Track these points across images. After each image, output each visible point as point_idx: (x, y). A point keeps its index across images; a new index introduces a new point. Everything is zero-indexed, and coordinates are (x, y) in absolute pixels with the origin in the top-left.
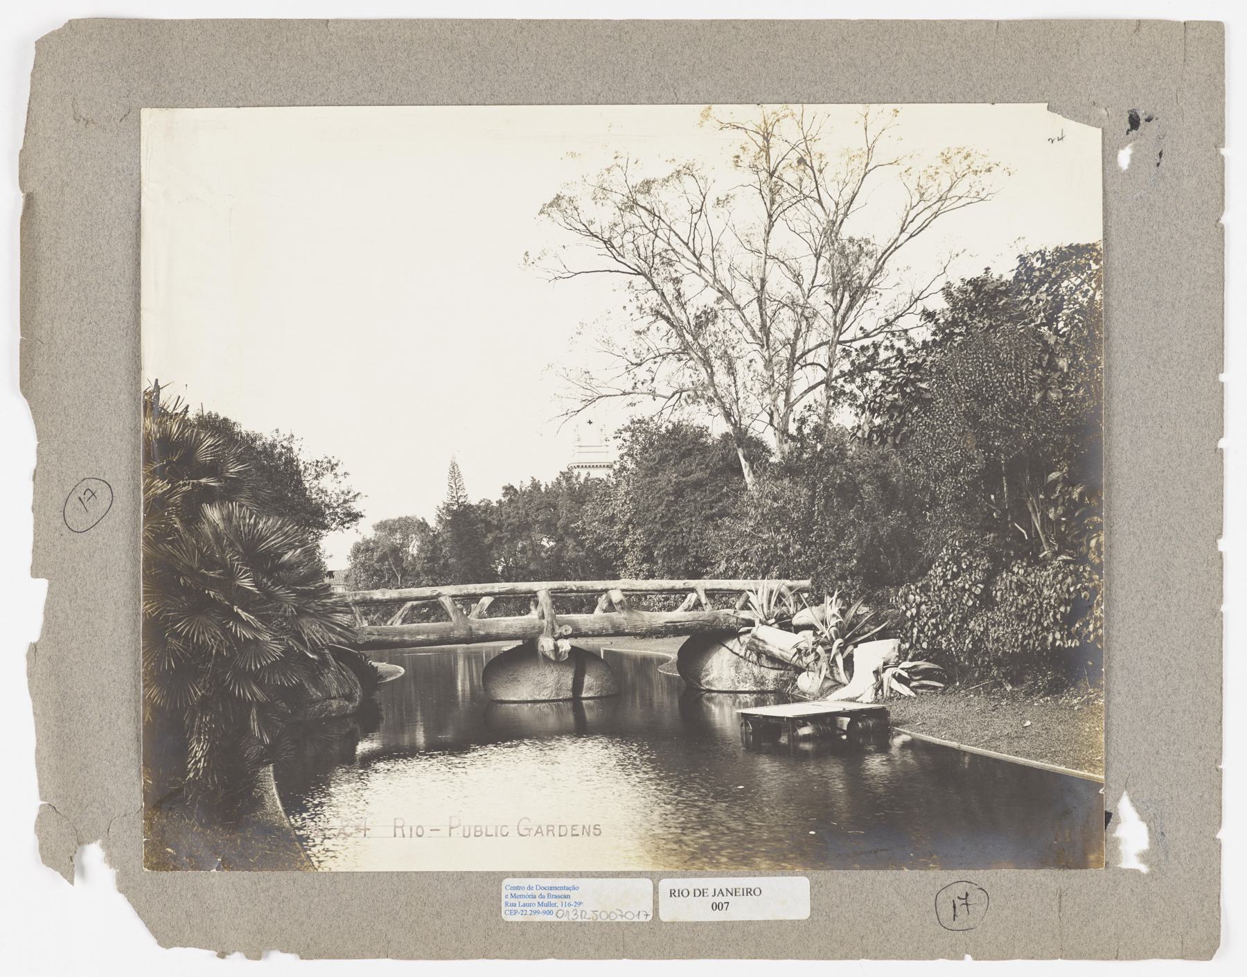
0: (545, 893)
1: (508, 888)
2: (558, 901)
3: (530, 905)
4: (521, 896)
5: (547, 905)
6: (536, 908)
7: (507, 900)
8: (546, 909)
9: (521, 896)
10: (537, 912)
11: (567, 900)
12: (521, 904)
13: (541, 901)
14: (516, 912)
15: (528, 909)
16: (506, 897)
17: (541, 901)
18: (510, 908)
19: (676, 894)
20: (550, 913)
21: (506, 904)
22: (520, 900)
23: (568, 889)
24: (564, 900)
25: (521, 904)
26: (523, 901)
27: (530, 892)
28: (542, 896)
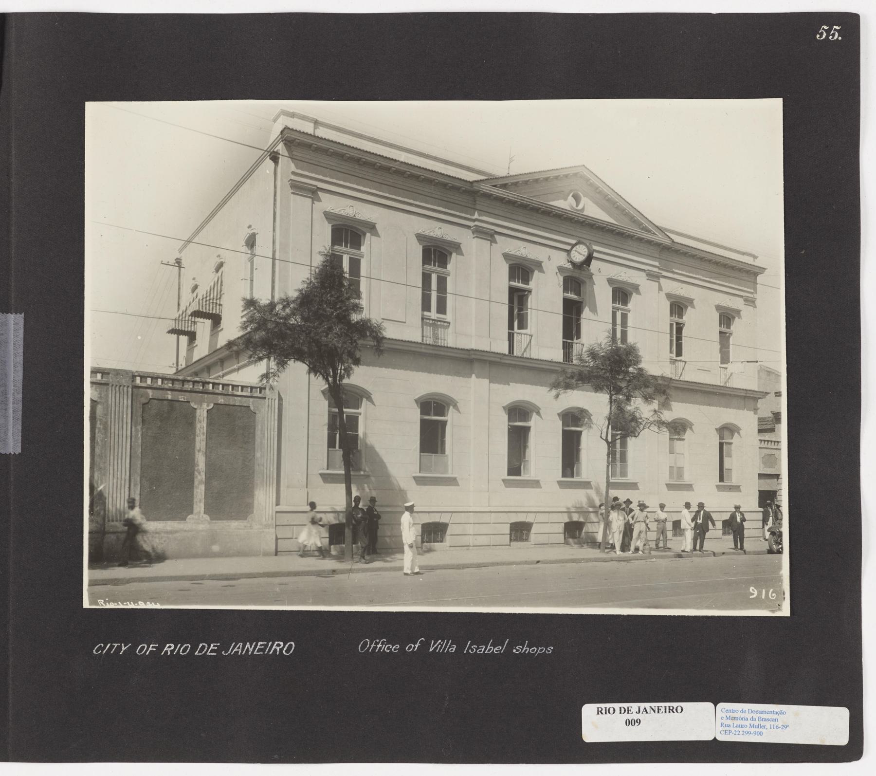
0: (756, 716)
1: (724, 710)
3: (742, 726)
7: (722, 721)
9: (734, 719)
11: (776, 723)
12: (735, 726)
14: (730, 732)
15: (741, 729)
16: (722, 718)
17: (752, 722)
20: (760, 734)
21: (722, 725)
23: (776, 713)
24: (773, 723)
25: (735, 726)
27: (743, 715)
28: (753, 719)
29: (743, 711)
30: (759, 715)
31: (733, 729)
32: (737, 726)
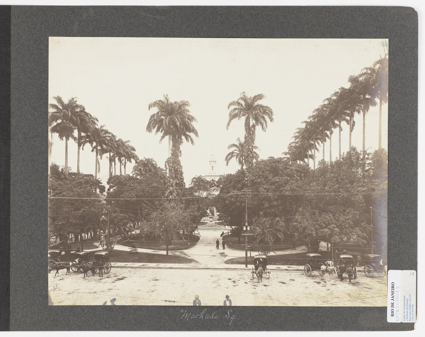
0: (406, 307)
2: (409, 303)
3: (410, 313)
4: (407, 316)
5: (410, 306)
6: (411, 310)
7: (408, 321)
8: (411, 307)
9: (407, 316)
11: (409, 299)
12: (410, 315)
13: (409, 309)
14: (412, 317)
15: (411, 313)
16: (407, 321)
17: (409, 309)
18: (411, 320)
19: (393, 314)
20: (413, 305)
21: (410, 321)
22: (408, 316)
23: (405, 299)
24: (409, 301)
25: (410, 315)
27: (406, 312)
28: (407, 308)
30: (406, 306)
31: (411, 317)
32: (410, 314)
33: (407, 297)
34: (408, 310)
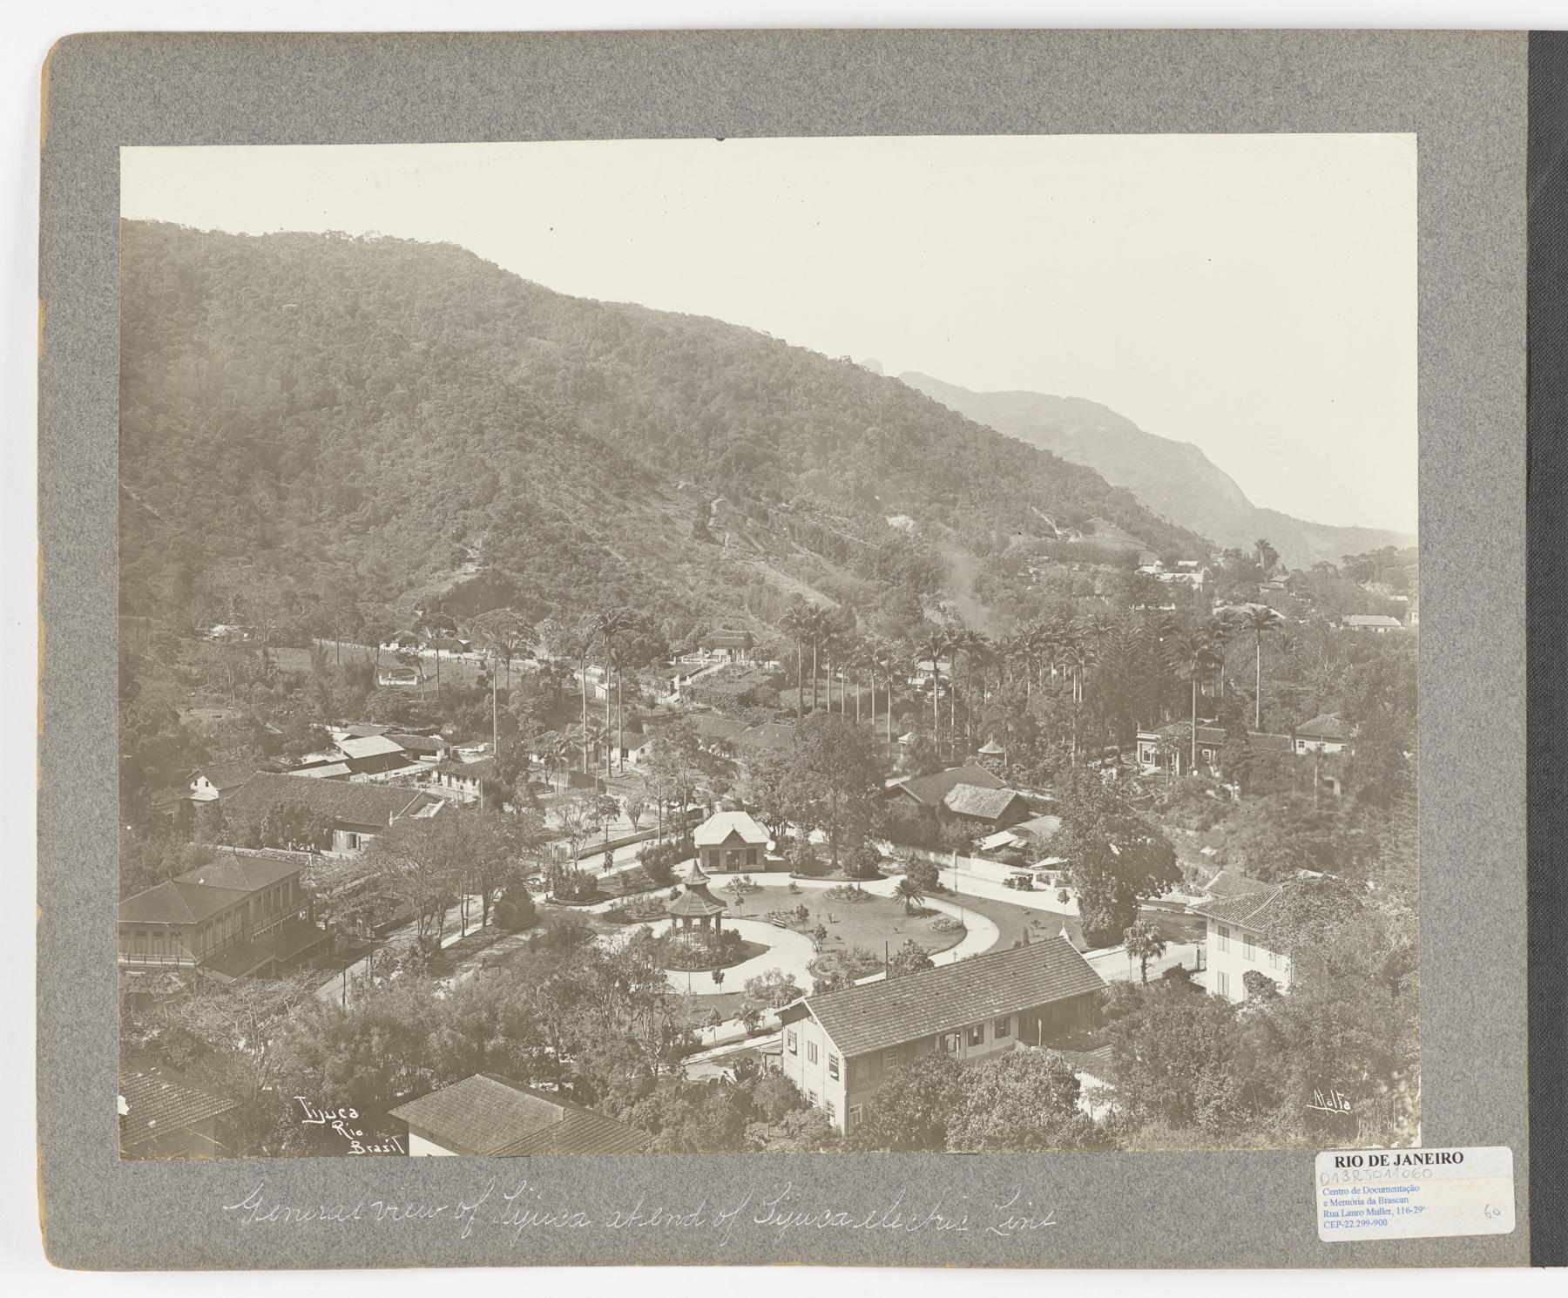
0: (1375, 1196)
2: (1393, 1207)
3: (1356, 1213)
5: (1378, 1213)
6: (1365, 1217)
10: (1366, 1222)
11: (1405, 1205)
13: (1370, 1207)
14: (1339, 1223)
15: (1354, 1219)
20: (1384, 1222)
21: (1326, 1214)
23: (1405, 1190)
24: (1400, 1205)
26: (1348, 1208)
27: (1356, 1197)
28: (1372, 1202)
29: (1355, 1191)
30: (1380, 1195)
32: (1349, 1214)
33: (1414, 1199)
34: (1367, 1206)
